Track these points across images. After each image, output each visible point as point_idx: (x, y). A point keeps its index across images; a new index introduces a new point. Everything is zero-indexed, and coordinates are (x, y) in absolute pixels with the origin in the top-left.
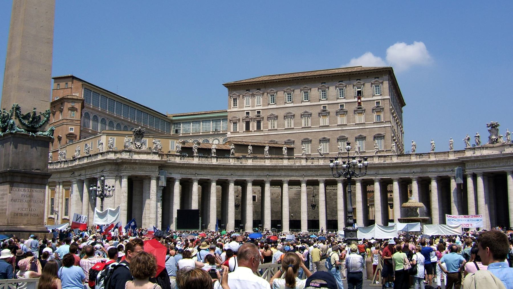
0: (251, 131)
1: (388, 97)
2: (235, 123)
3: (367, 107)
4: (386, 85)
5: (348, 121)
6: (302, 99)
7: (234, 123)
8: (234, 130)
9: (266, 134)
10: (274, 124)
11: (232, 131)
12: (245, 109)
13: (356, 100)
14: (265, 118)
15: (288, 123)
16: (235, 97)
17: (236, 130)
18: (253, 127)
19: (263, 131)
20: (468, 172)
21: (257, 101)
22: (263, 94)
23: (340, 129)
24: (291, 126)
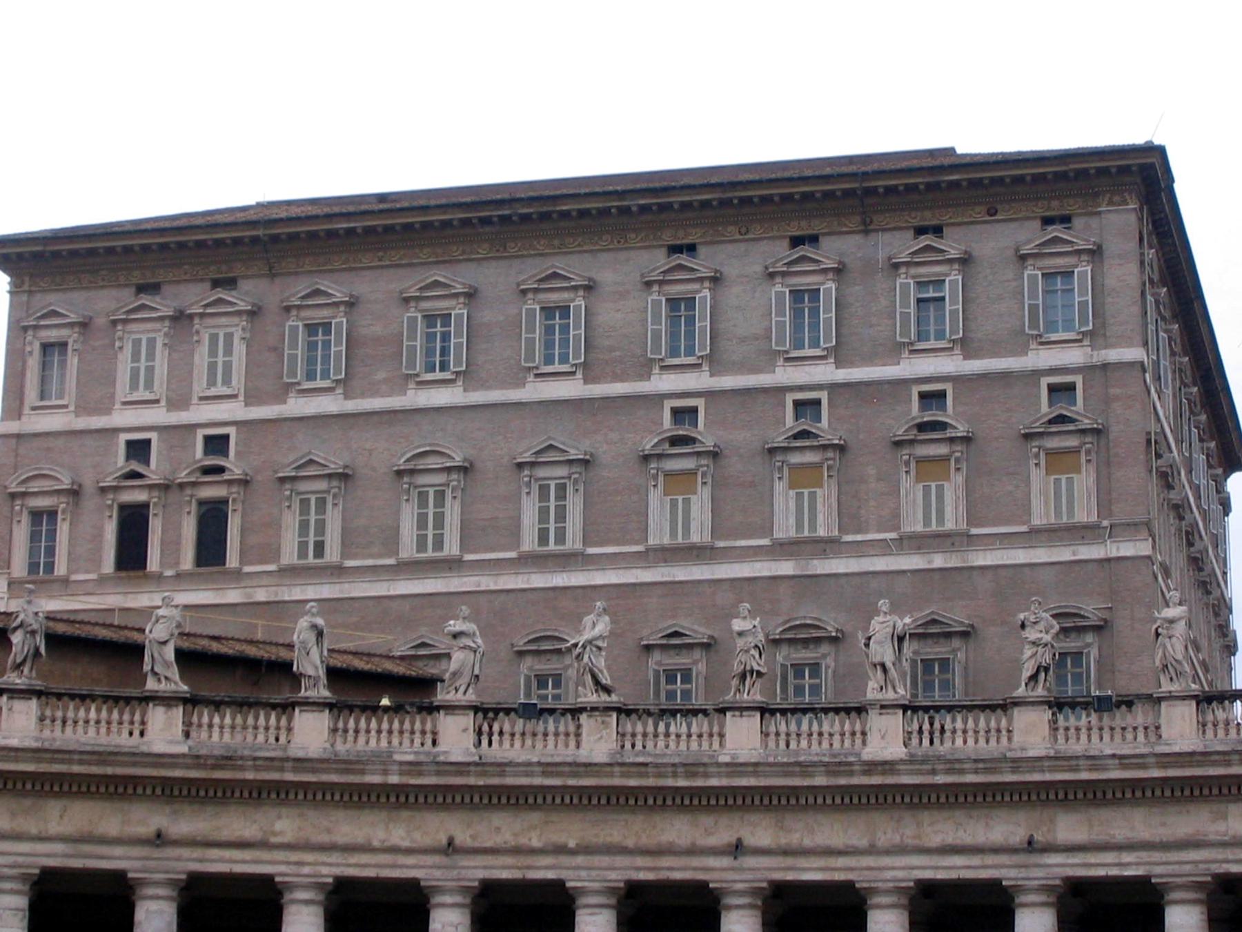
0: (159, 578)
2: (43, 519)
5: (848, 518)
6: (530, 357)
7: (36, 515)
8: (33, 567)
9: (261, 595)
10: (321, 527)
11: (19, 568)
12: (122, 418)
15: (422, 522)
16: (53, 335)
17: (50, 567)
18: (171, 547)
21: (212, 367)
23: (786, 568)
24: (439, 543)
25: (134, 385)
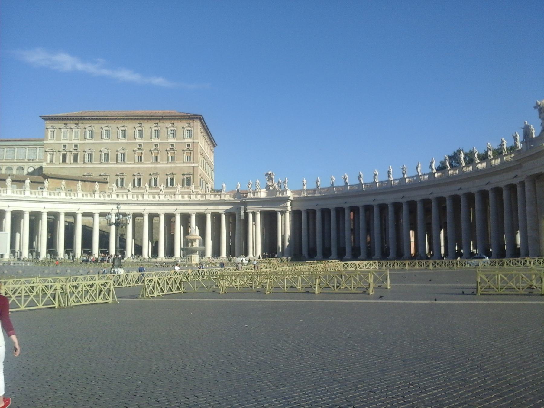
20: (248, 210)
25: (64, 137)
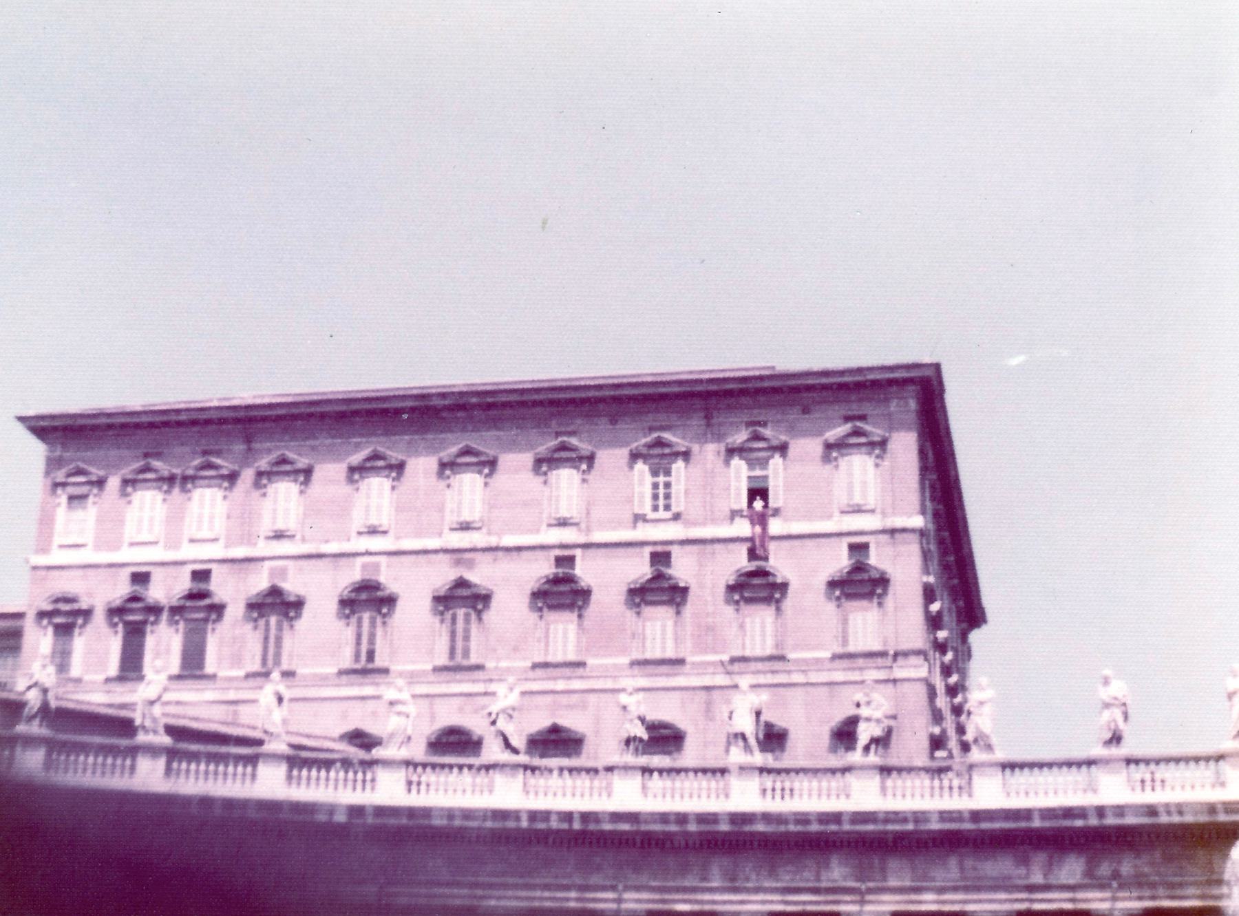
1: (918, 521)
2: (64, 631)
3: (806, 570)
4: (905, 446)
13: (743, 528)
14: (235, 611)
19: (213, 677)
22: (232, 477)
